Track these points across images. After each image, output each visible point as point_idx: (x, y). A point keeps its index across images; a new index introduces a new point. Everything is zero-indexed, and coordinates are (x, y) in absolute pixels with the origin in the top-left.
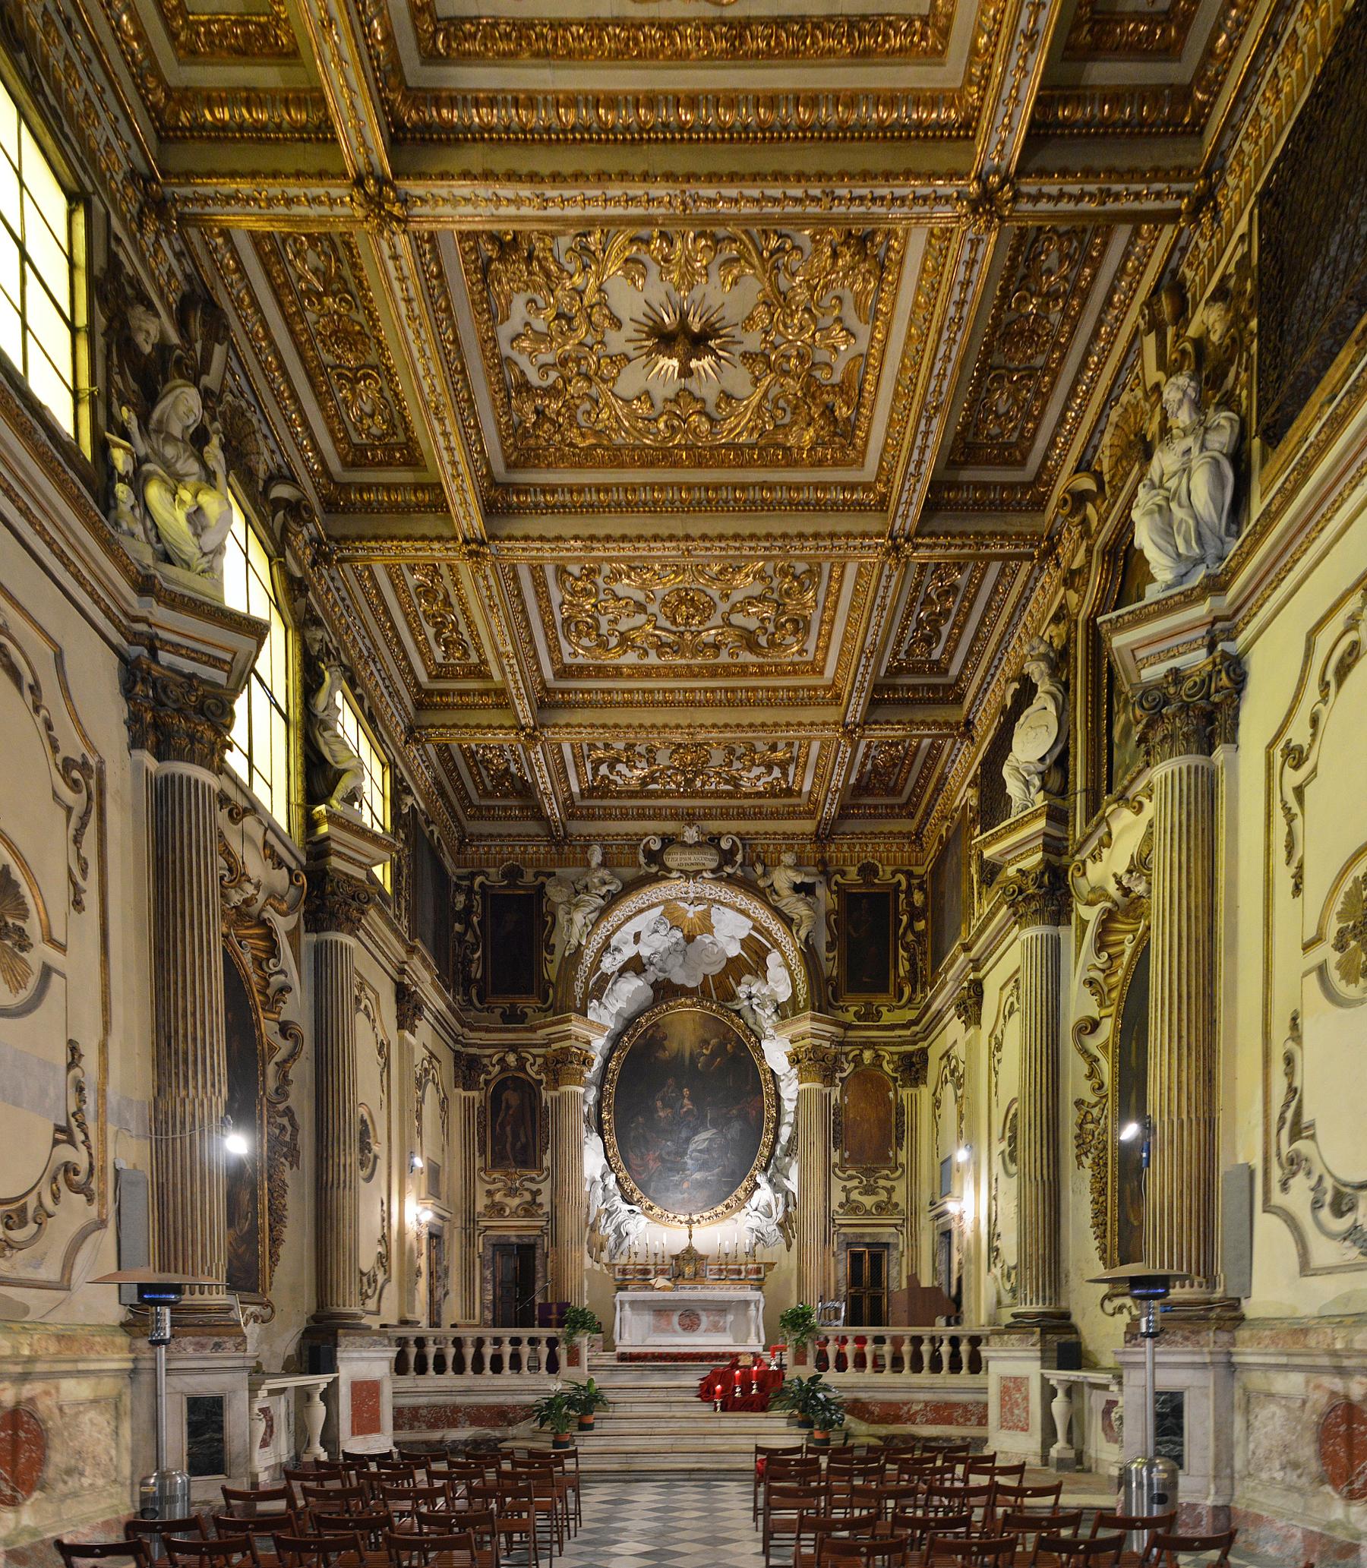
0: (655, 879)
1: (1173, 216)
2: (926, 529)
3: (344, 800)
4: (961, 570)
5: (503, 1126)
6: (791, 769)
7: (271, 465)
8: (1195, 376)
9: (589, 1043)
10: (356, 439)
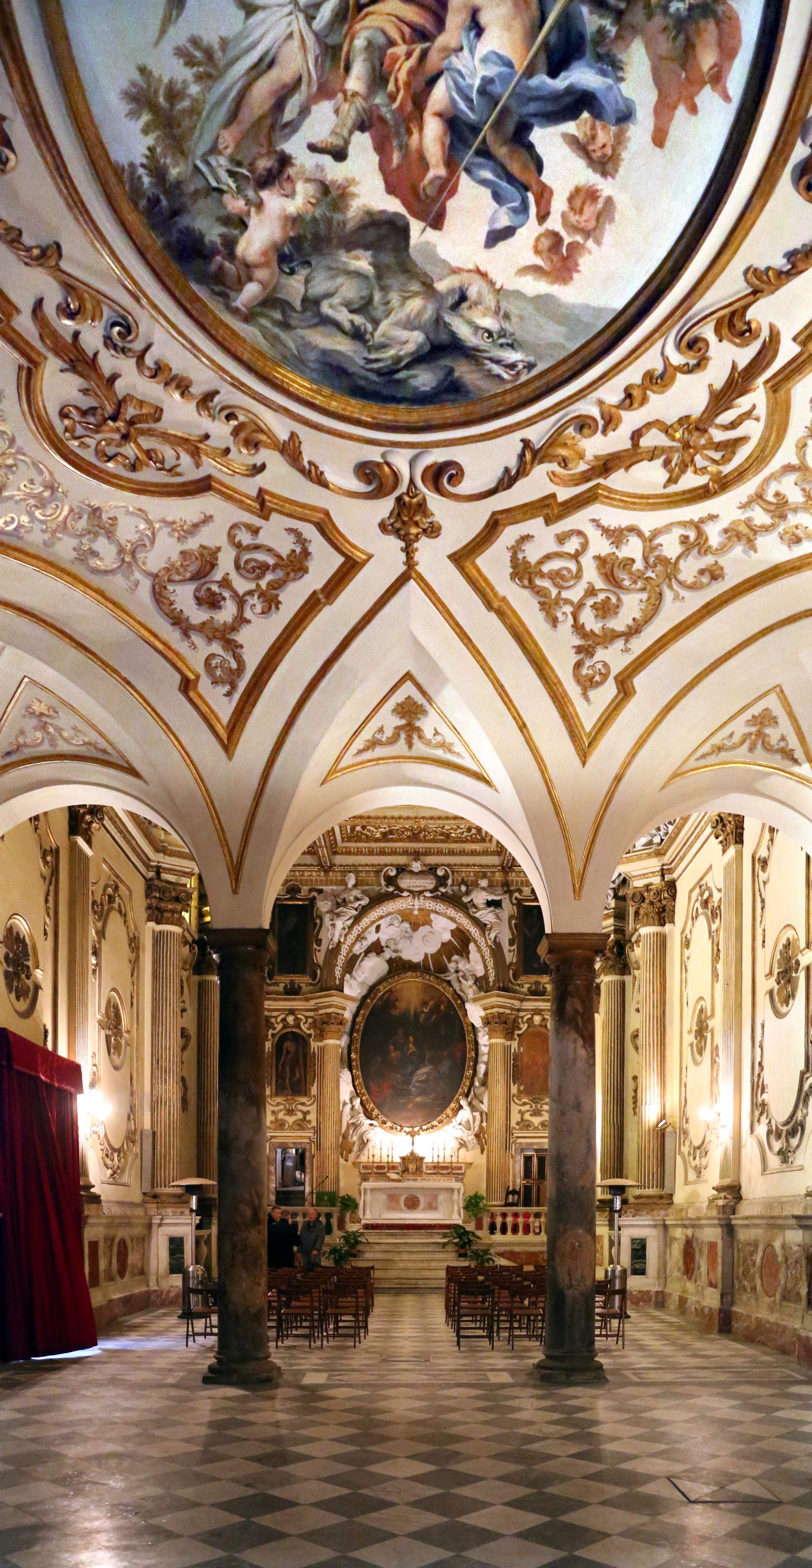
0: (391, 897)
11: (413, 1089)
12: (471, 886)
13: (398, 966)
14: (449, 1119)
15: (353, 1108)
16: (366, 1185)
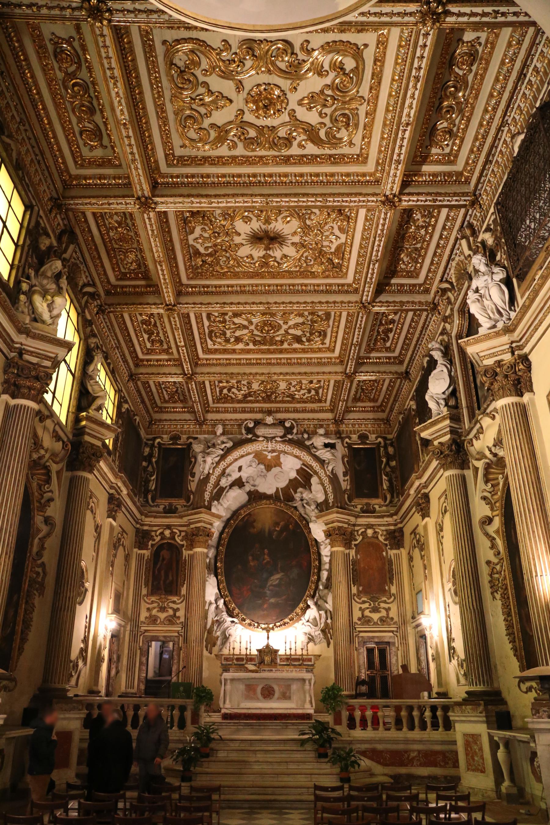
2: (377, 300)
9: (211, 524)
13: (255, 497)
14: (299, 617)
15: (217, 607)
16: (226, 675)
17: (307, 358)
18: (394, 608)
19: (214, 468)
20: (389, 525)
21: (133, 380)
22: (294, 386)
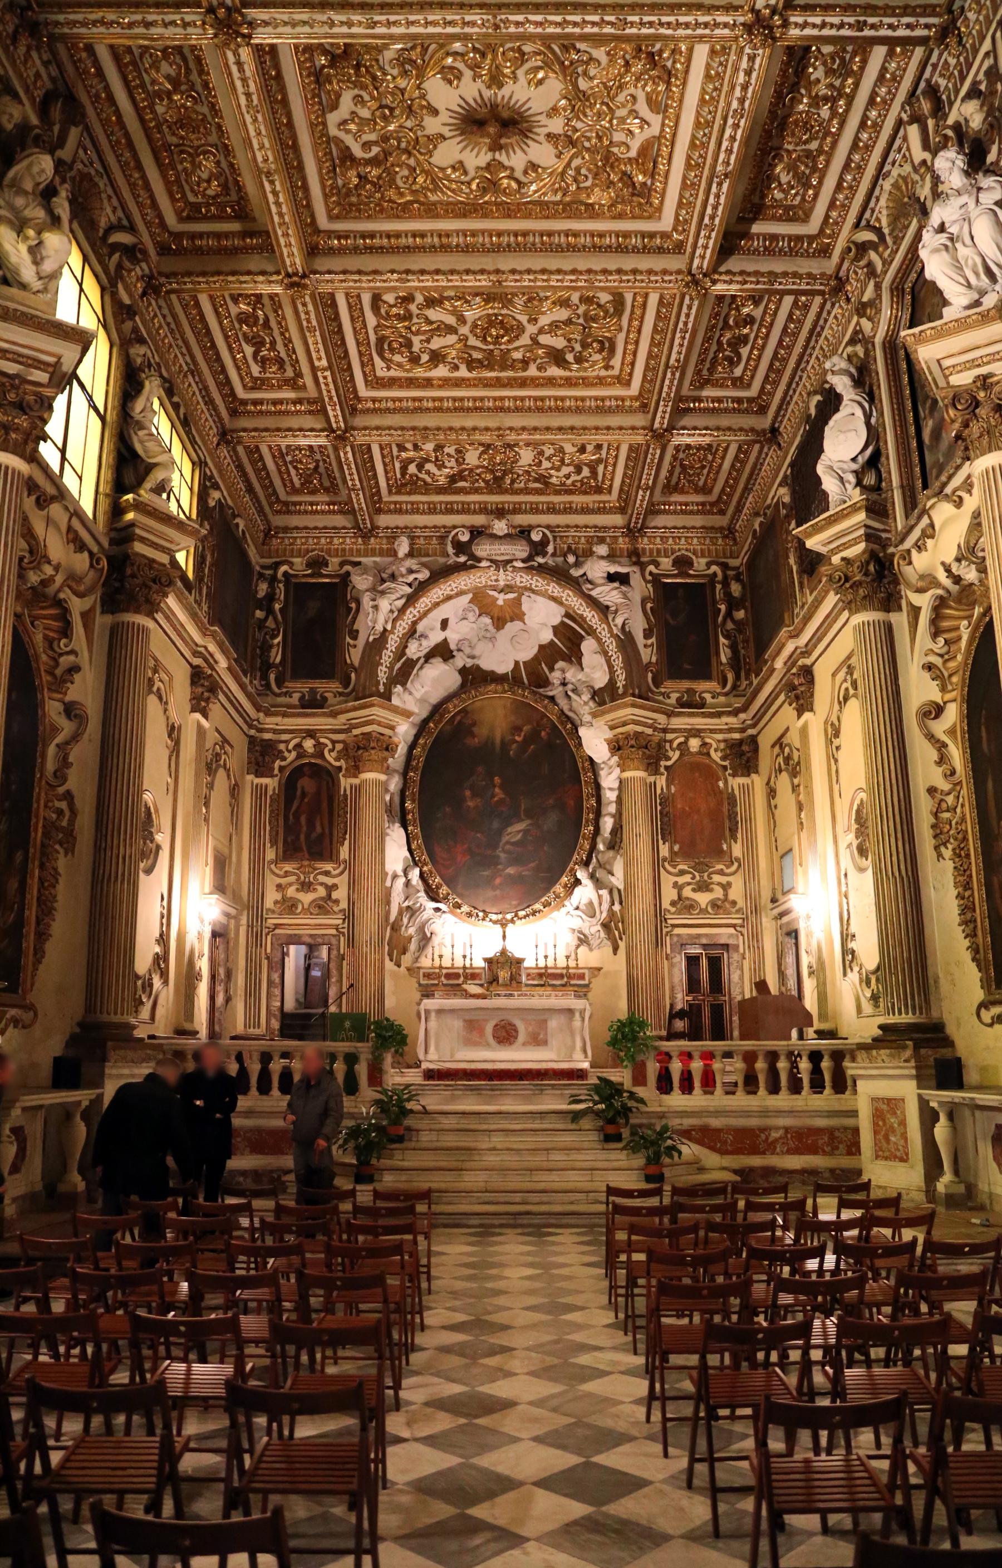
1: (923, 41)
3: (152, 490)
4: (756, 303)
5: (297, 816)
6: (601, 469)
7: (113, 218)
8: (961, 150)
9: (392, 728)
10: (192, 199)
11: (502, 855)
12: (585, 554)
13: (474, 678)
14: (560, 900)
15: (408, 884)
16: (428, 1003)
17: (576, 399)
18: (737, 884)
19: (395, 621)
20: (730, 730)
21: (228, 443)
22: (549, 459)
